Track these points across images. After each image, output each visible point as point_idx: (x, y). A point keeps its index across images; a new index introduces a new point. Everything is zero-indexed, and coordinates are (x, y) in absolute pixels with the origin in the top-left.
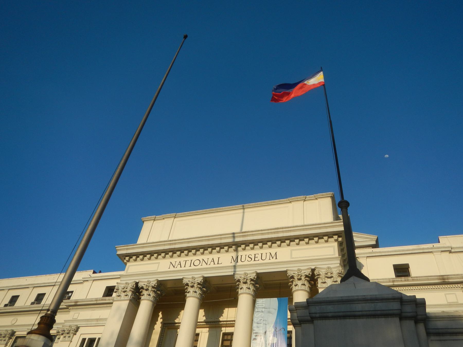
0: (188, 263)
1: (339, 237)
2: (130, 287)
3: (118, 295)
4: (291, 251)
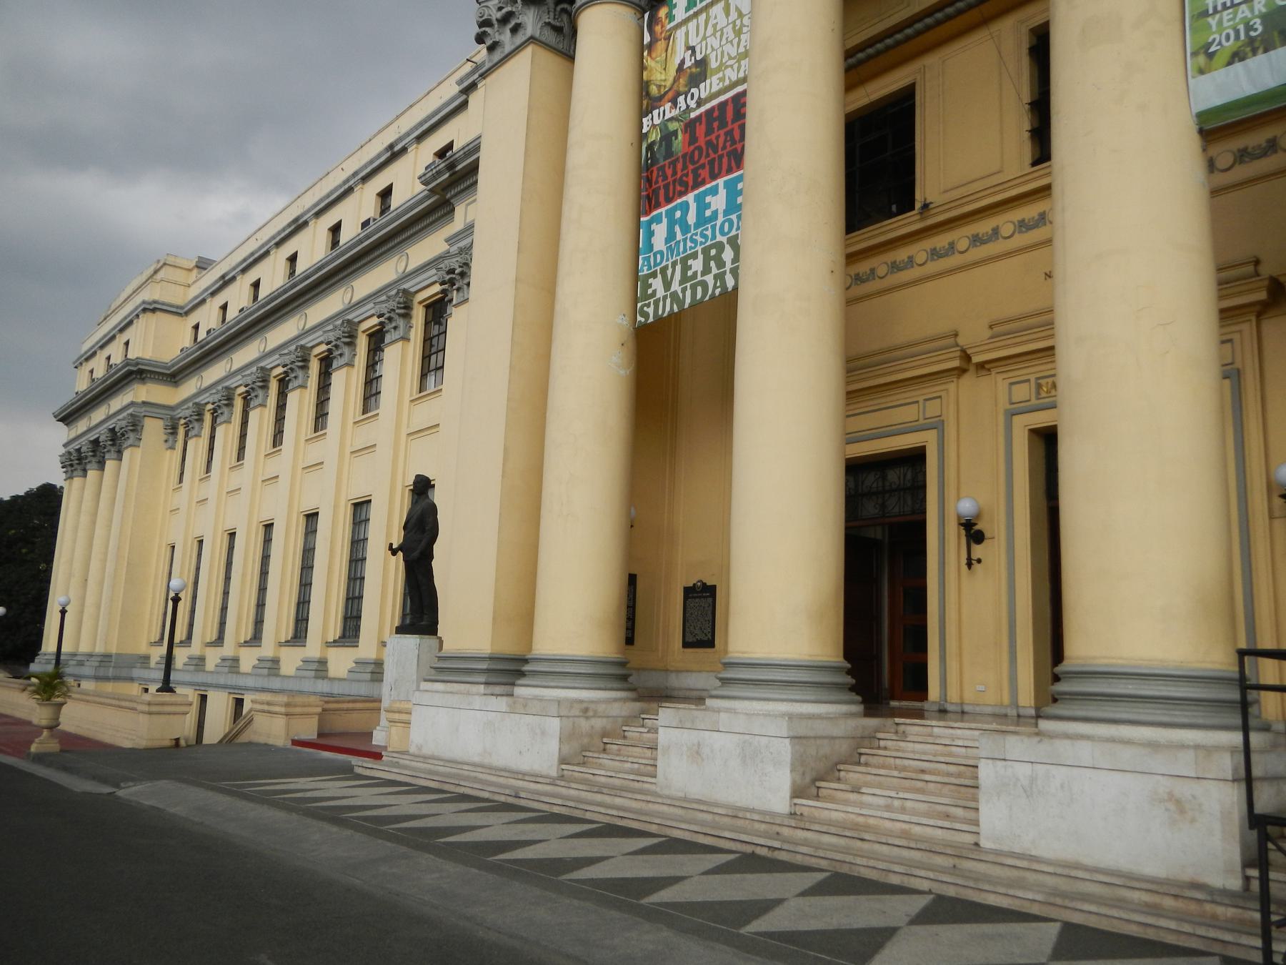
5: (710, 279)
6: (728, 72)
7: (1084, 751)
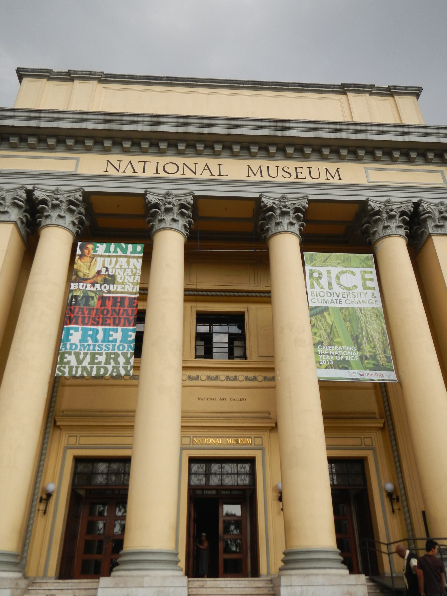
5: (110, 367)
6: (127, 287)
7: (320, 580)
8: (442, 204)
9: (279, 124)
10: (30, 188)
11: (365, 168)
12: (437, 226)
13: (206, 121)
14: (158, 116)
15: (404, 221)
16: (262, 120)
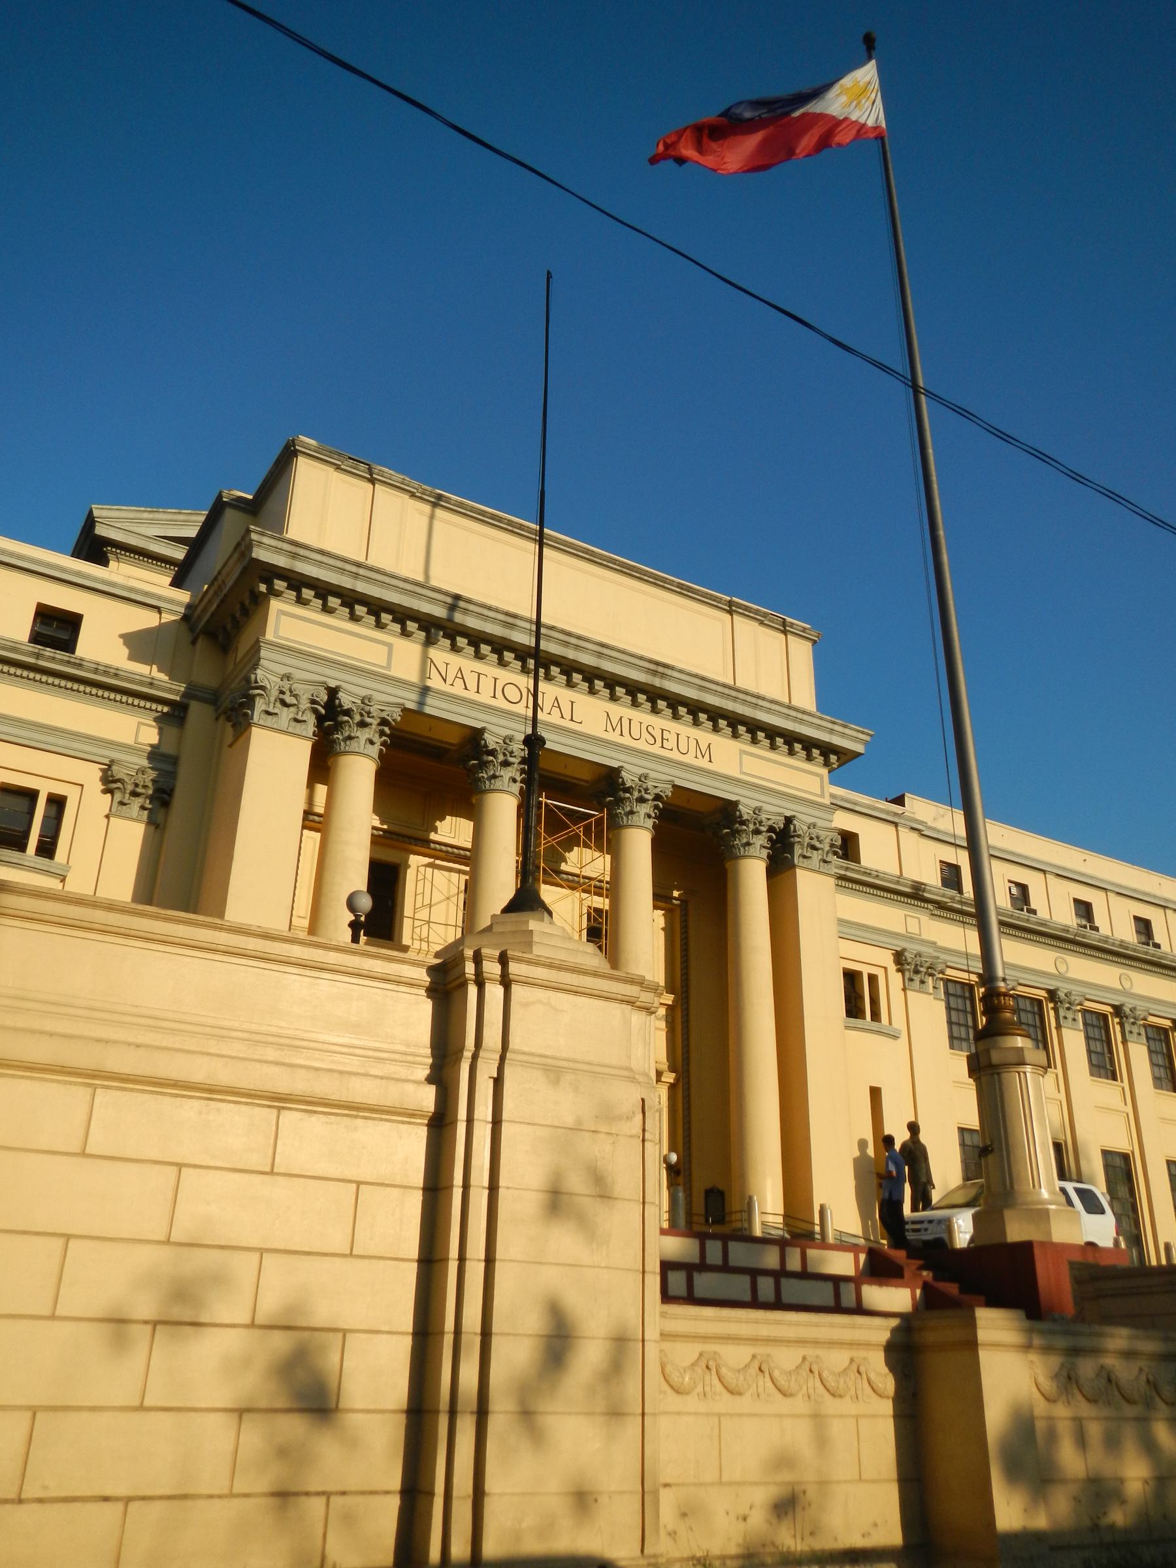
0: (487, 685)
1: (839, 759)
2: (305, 694)
3: (264, 707)
4: (742, 752)
8: (814, 826)
9: (660, 669)
10: (333, 684)
11: (742, 752)
12: (805, 857)
13: (573, 641)
14: (515, 616)
15: (770, 839)
16: (641, 658)
